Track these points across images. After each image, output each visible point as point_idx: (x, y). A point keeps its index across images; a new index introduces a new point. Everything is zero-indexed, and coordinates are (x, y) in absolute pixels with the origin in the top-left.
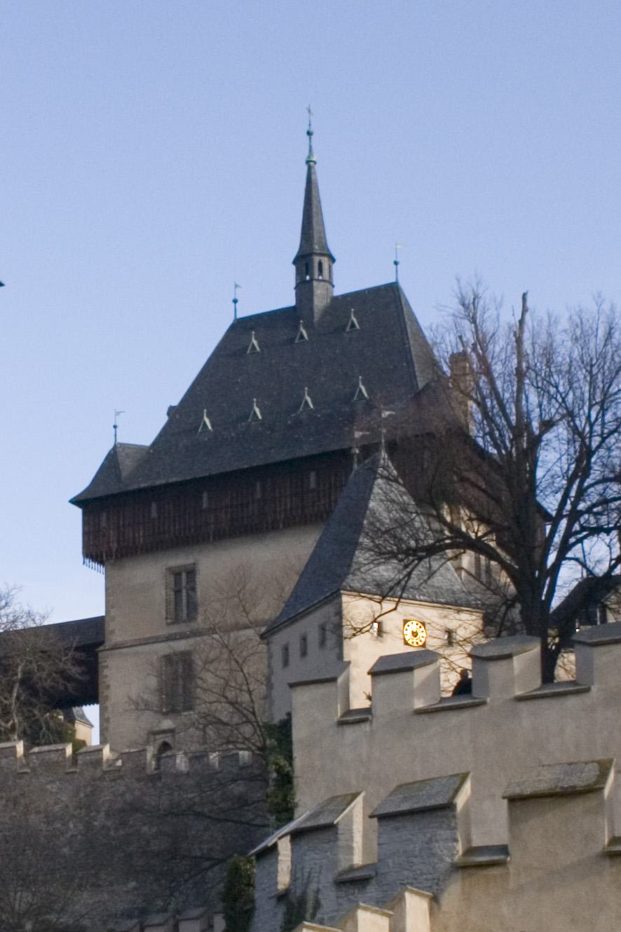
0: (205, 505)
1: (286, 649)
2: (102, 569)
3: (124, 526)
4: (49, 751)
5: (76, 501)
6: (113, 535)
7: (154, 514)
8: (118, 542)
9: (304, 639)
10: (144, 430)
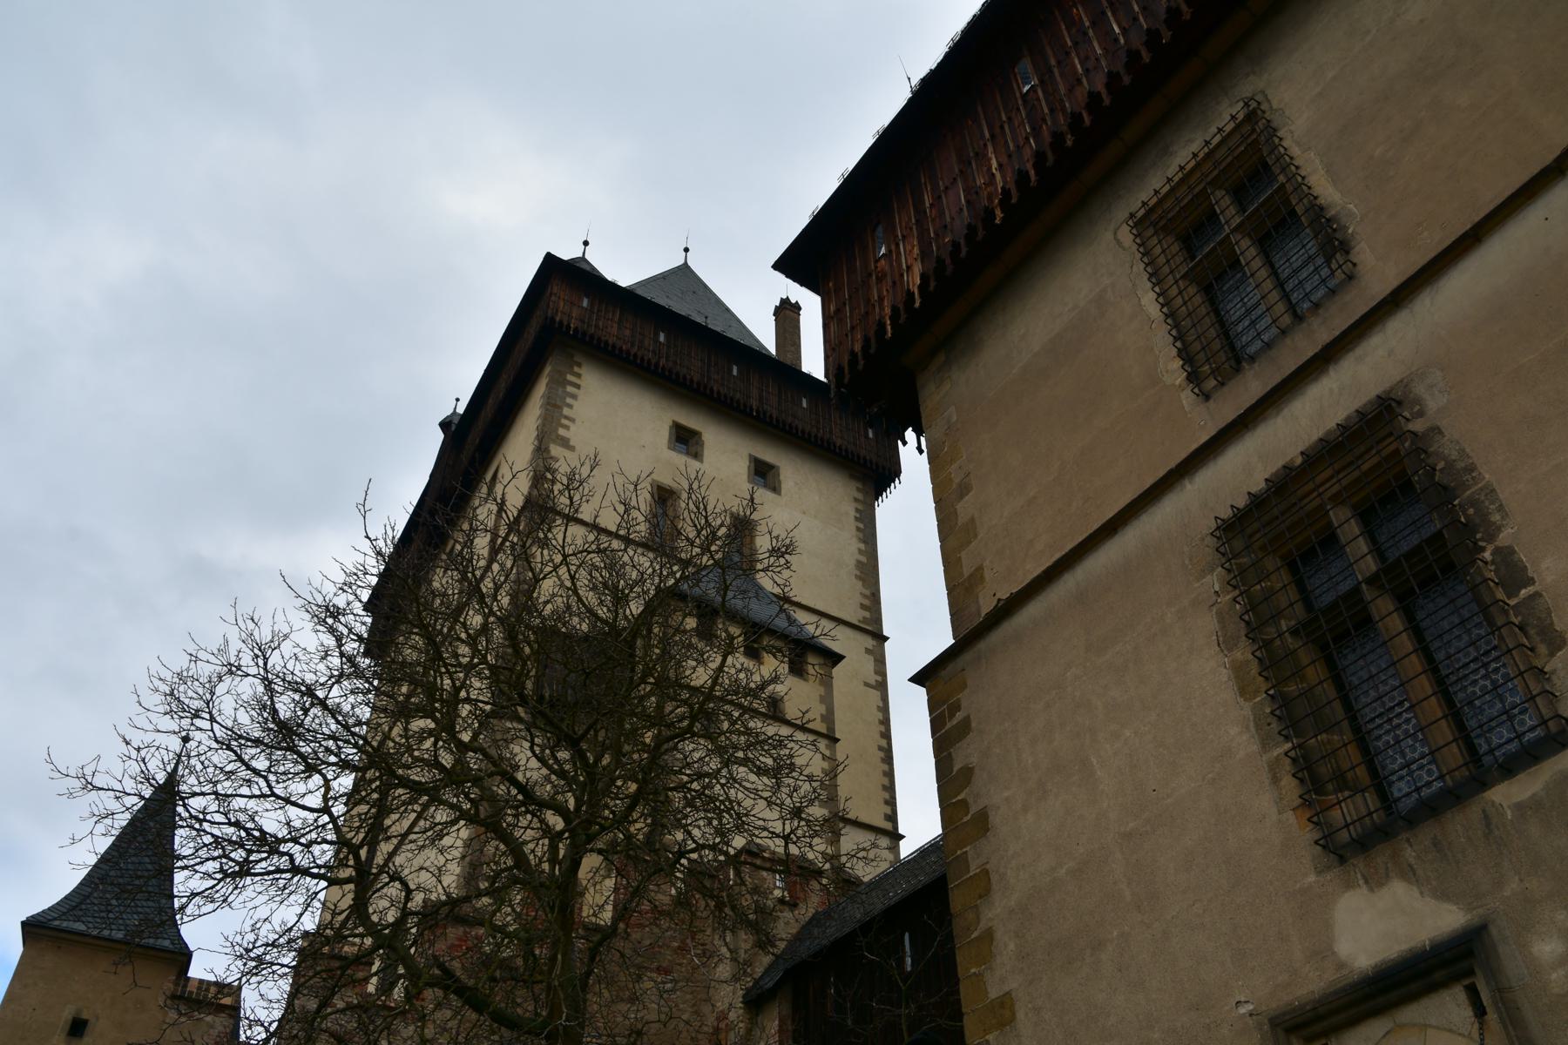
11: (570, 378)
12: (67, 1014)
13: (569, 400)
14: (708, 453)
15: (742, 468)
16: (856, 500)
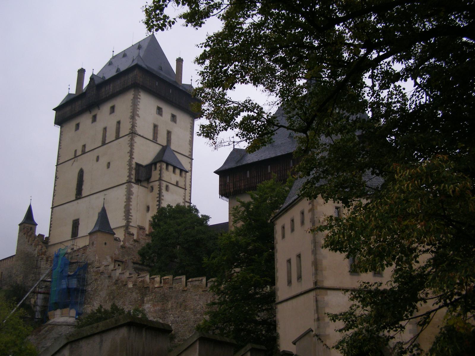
1: (283, 227)
2: (228, 200)
3: (236, 181)
4: (196, 281)
5: (216, 172)
7: (248, 176)
8: (233, 189)
9: (293, 221)
11: (139, 97)
12: (104, 242)
13: (139, 103)
14: (164, 113)
15: (169, 117)
16: (191, 123)
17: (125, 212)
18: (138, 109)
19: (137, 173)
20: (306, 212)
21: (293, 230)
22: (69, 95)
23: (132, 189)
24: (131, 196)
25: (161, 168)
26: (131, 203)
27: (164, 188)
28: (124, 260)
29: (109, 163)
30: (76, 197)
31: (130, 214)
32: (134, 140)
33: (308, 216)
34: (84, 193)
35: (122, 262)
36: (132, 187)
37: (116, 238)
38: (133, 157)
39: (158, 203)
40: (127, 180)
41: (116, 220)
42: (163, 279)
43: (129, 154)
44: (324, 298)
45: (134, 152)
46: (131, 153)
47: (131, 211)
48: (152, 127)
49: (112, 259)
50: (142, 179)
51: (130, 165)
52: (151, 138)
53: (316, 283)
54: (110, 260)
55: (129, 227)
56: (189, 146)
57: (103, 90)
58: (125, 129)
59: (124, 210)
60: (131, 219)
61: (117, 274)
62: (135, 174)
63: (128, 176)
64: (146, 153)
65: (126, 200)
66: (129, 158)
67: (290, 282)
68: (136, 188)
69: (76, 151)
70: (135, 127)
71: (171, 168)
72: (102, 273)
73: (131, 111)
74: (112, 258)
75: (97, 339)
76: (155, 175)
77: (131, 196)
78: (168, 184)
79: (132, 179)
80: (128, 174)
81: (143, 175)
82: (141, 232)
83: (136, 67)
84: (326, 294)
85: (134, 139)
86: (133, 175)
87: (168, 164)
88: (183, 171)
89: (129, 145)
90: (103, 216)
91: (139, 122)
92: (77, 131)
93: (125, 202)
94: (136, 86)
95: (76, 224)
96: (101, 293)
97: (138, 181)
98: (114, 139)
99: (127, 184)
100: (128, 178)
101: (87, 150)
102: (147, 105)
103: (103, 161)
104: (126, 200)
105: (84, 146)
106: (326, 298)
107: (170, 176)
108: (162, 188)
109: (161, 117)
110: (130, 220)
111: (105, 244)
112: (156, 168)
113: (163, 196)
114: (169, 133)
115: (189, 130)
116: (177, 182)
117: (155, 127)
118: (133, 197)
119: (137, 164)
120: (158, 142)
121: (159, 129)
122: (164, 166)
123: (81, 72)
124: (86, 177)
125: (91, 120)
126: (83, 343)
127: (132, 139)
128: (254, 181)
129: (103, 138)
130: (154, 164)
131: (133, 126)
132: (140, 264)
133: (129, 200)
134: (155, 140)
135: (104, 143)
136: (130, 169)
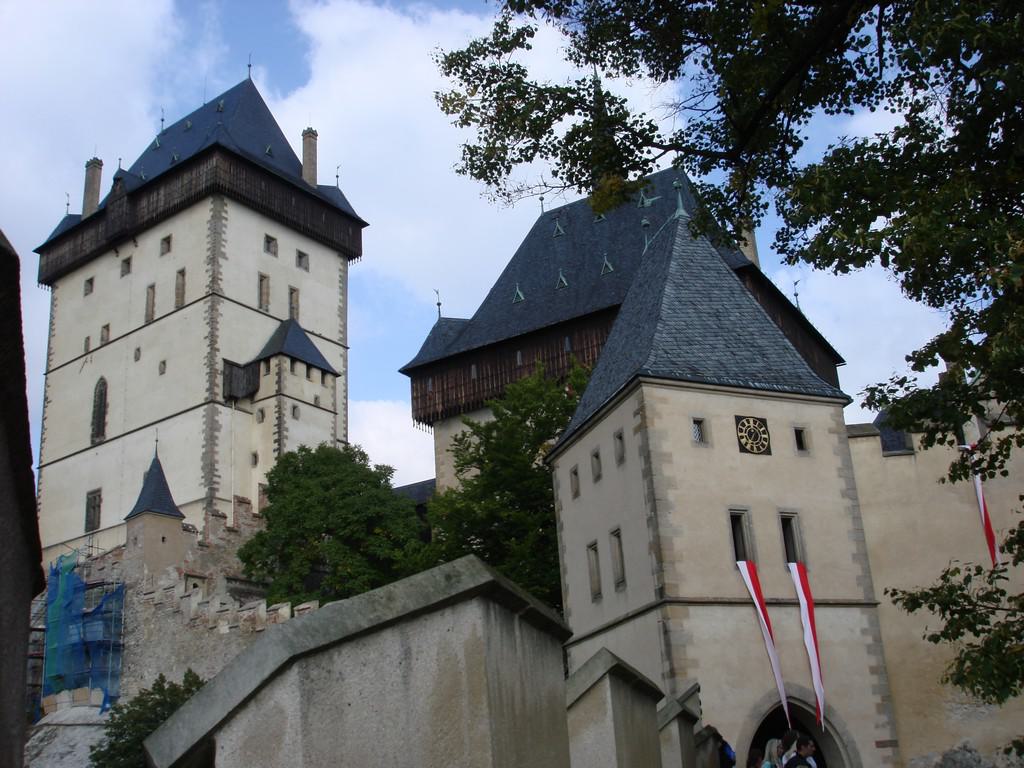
0: (519, 363)
3: (448, 388)
5: (405, 371)
6: (438, 399)
7: (474, 375)
8: (443, 404)
10: (465, 307)
11: (224, 214)
13: (224, 229)
15: (293, 257)
16: (340, 270)
17: (203, 469)
18: (223, 243)
19: (229, 380)
20: (628, 435)
21: (598, 477)
22: (70, 218)
23: (216, 418)
24: (217, 434)
25: (280, 369)
26: (216, 449)
27: (288, 413)
28: (207, 574)
29: (164, 363)
30: (93, 442)
31: (216, 473)
32: (217, 310)
33: (632, 442)
34: (110, 432)
35: (202, 578)
36: (217, 412)
37: (188, 525)
38: (217, 346)
39: (276, 446)
40: (206, 399)
41: (184, 487)
42: (299, 610)
43: (208, 342)
44: (682, 626)
45: (217, 336)
46: (212, 339)
47: (217, 466)
48: (256, 280)
49: (180, 574)
50: (240, 394)
51: (211, 364)
52: (255, 304)
53: (661, 591)
54: (175, 575)
55: (215, 501)
56: (338, 319)
57: (144, 203)
58: (197, 285)
59: (201, 464)
60: (218, 483)
61: (194, 605)
62: (224, 384)
63: (207, 390)
64: (247, 337)
65: (204, 443)
66: (208, 349)
67: (597, 596)
68: (226, 415)
69: (88, 338)
70: (220, 282)
71: (301, 368)
72: (159, 605)
73: (209, 246)
74: (178, 570)
75: (390, 640)
76: (267, 384)
77: (217, 434)
78: (296, 403)
79: (217, 394)
80: (207, 385)
81: (239, 385)
82: (242, 509)
83: (216, 148)
84: (687, 616)
85: (218, 307)
86: (217, 386)
87: (294, 360)
88: (327, 371)
89: (208, 321)
90: (155, 479)
91: (227, 270)
92: (88, 297)
93: (203, 447)
94: (216, 191)
95: (94, 501)
96: (158, 650)
97: (231, 399)
98: (173, 309)
99: (206, 407)
100: (207, 395)
101: (112, 337)
102: (244, 229)
103: (150, 359)
104: (204, 443)
105: (107, 327)
106: (687, 624)
107: (301, 384)
108: (284, 412)
109: (274, 259)
110: (216, 486)
111: (163, 538)
112: (268, 369)
113: (287, 430)
114: (293, 291)
115: (337, 284)
116: (316, 398)
117: (263, 278)
118: (221, 435)
119: (226, 361)
120: (271, 313)
121: (271, 283)
122: (287, 363)
123: (95, 165)
124: (111, 398)
125: (118, 271)
126: (344, 660)
127: (213, 308)
128: (488, 385)
129: (147, 310)
130: (265, 358)
131: (215, 279)
132: (242, 581)
133: (211, 440)
134: (262, 309)
135: (150, 320)
136: (212, 374)
